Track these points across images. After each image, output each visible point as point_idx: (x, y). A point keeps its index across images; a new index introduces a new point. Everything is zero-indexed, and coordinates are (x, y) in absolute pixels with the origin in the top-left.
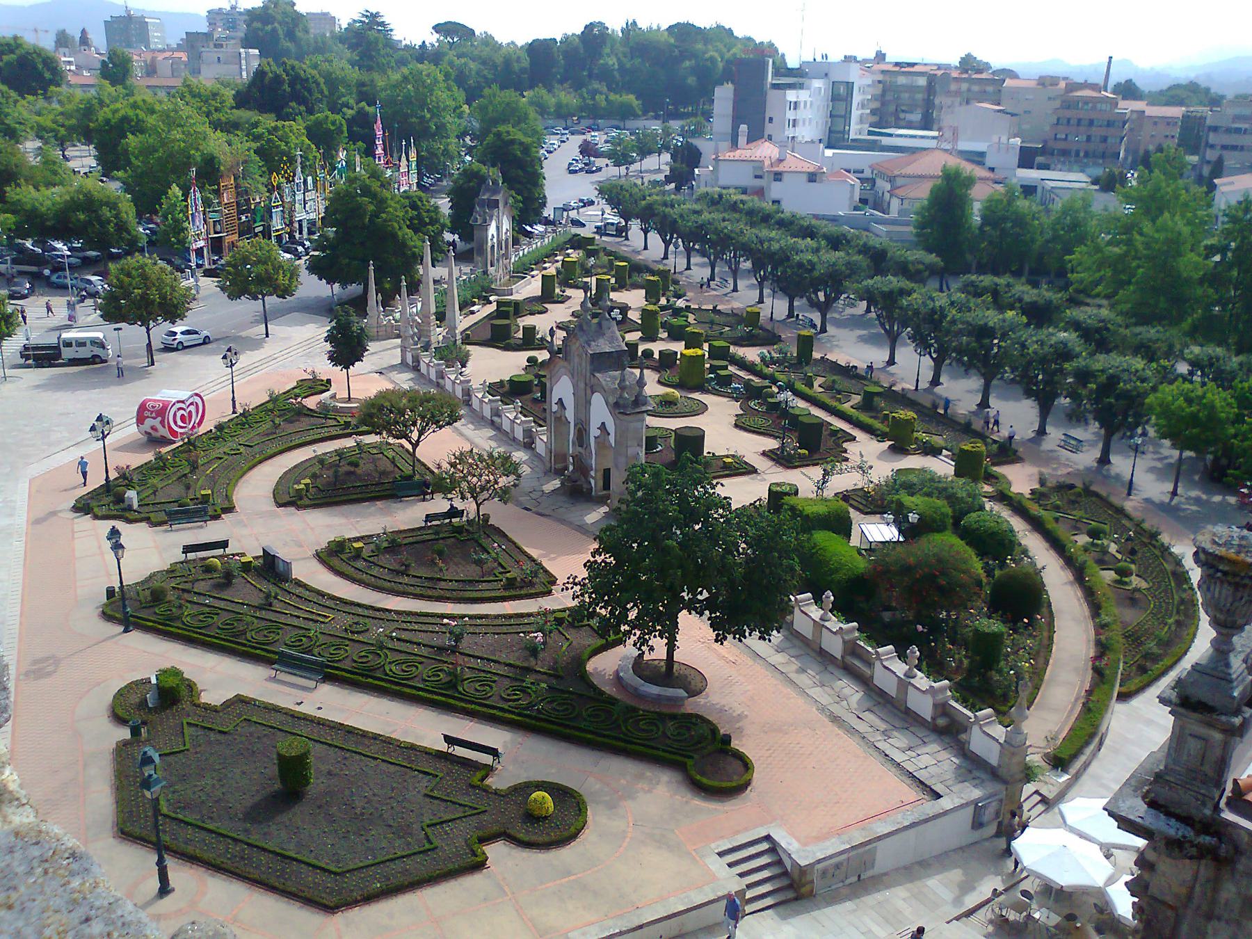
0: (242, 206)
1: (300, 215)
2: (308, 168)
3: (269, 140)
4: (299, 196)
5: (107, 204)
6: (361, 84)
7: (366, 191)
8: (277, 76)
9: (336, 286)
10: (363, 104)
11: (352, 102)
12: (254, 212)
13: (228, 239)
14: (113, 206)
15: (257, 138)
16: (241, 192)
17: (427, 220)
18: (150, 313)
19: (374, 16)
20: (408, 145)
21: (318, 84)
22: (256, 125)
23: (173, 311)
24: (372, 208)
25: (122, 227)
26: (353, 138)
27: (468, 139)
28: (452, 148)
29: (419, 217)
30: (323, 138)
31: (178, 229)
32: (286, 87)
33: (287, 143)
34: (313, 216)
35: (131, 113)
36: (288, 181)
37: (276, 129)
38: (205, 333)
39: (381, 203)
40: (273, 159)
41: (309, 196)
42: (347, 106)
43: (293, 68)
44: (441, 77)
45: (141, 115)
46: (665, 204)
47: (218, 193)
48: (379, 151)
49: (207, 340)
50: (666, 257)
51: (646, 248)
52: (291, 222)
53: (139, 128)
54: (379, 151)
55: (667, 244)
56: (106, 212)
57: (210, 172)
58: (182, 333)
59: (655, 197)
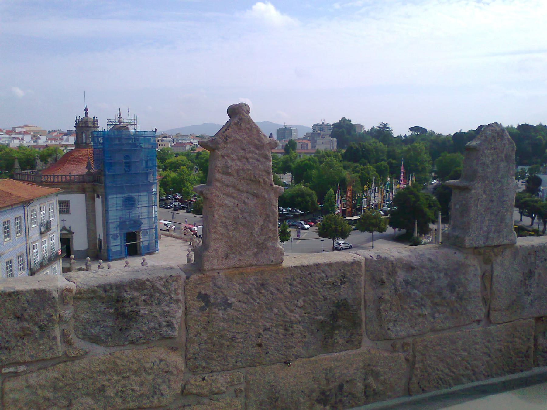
0: (353, 198)
1: (372, 202)
2: (377, 185)
3: (362, 173)
4: (373, 195)
5: (308, 195)
6: (389, 152)
7: (412, 193)
8: (357, 149)
9: (397, 229)
10: (390, 159)
11: (386, 158)
12: (357, 200)
13: (348, 210)
14: (311, 196)
15: (358, 172)
16: (354, 193)
17: (432, 205)
18: (337, 235)
19: (385, 125)
20: (412, 176)
21: (373, 152)
22: (356, 167)
23: (344, 235)
24: (414, 199)
25: (313, 203)
26: (391, 173)
27: (433, 174)
28: (428, 177)
29: (429, 204)
30: (381, 172)
31: (332, 205)
32: (361, 153)
33: (368, 174)
34: (377, 203)
35: (308, 162)
36: (369, 188)
37: (364, 169)
38: (350, 244)
39: (417, 197)
40: (364, 181)
41: (377, 194)
42: (383, 160)
43: (363, 145)
44: (424, 149)
45: (312, 163)
46: (533, 201)
47: (346, 192)
48: (402, 178)
49: (351, 247)
50: (532, 224)
51: (521, 220)
52: (369, 204)
53: (311, 167)
54: (402, 178)
55: (533, 218)
56: (308, 198)
57: (343, 185)
58: (343, 244)
59: (528, 199)
